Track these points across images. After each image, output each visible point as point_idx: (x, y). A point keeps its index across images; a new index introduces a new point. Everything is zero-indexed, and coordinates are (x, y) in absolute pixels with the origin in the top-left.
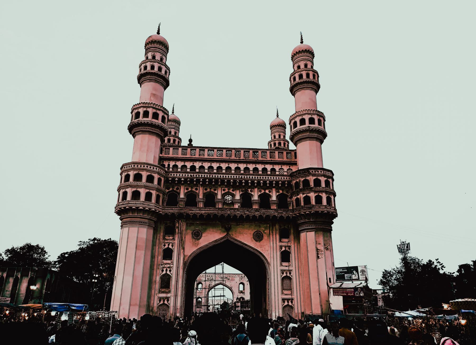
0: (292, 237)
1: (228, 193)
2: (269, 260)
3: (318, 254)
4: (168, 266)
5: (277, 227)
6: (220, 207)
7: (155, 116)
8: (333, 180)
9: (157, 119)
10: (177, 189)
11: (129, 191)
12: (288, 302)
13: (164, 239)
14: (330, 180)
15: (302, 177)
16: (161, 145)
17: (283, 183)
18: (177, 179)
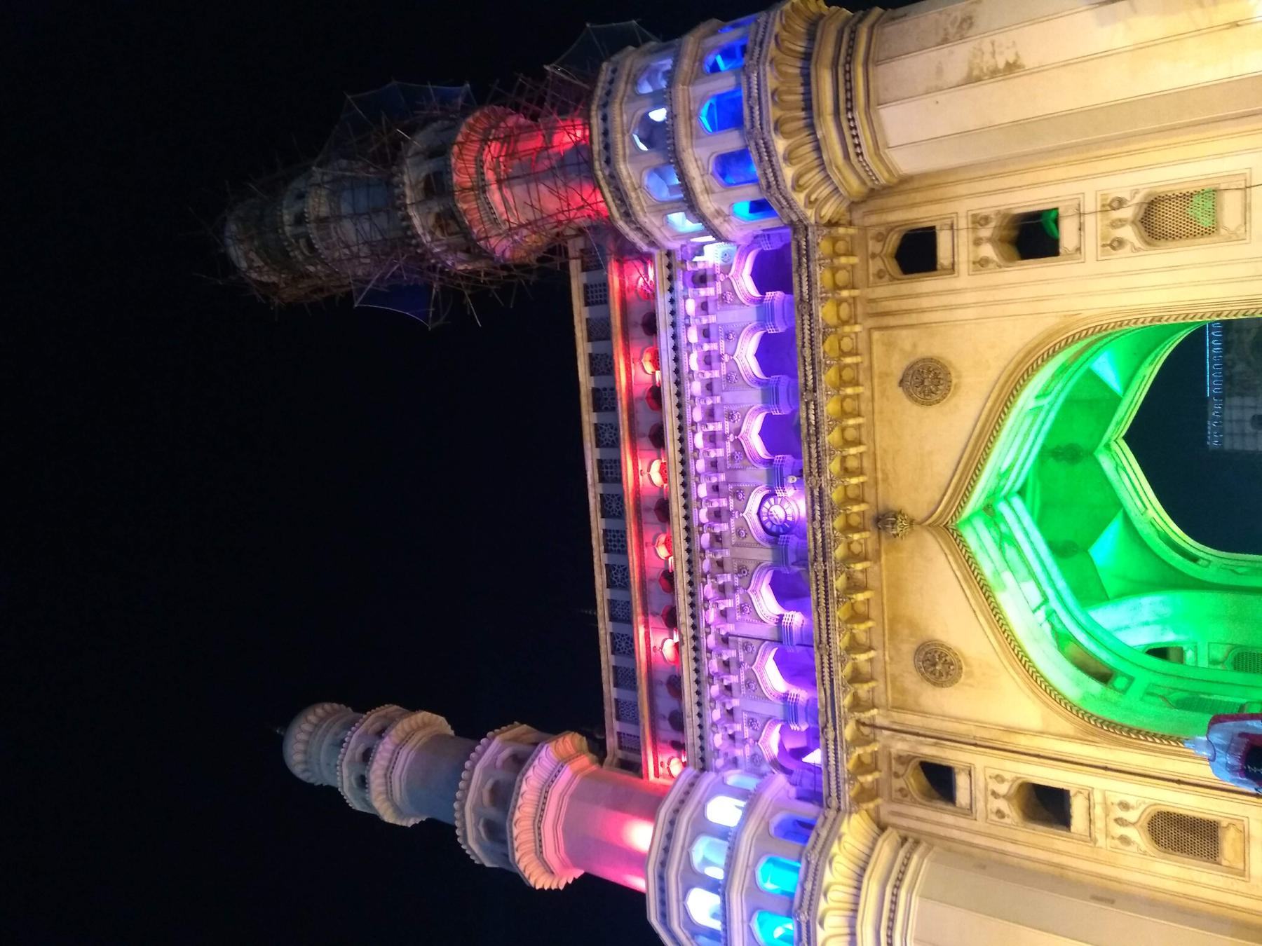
2: (1050, 322)
3: (994, 73)
5: (882, 291)
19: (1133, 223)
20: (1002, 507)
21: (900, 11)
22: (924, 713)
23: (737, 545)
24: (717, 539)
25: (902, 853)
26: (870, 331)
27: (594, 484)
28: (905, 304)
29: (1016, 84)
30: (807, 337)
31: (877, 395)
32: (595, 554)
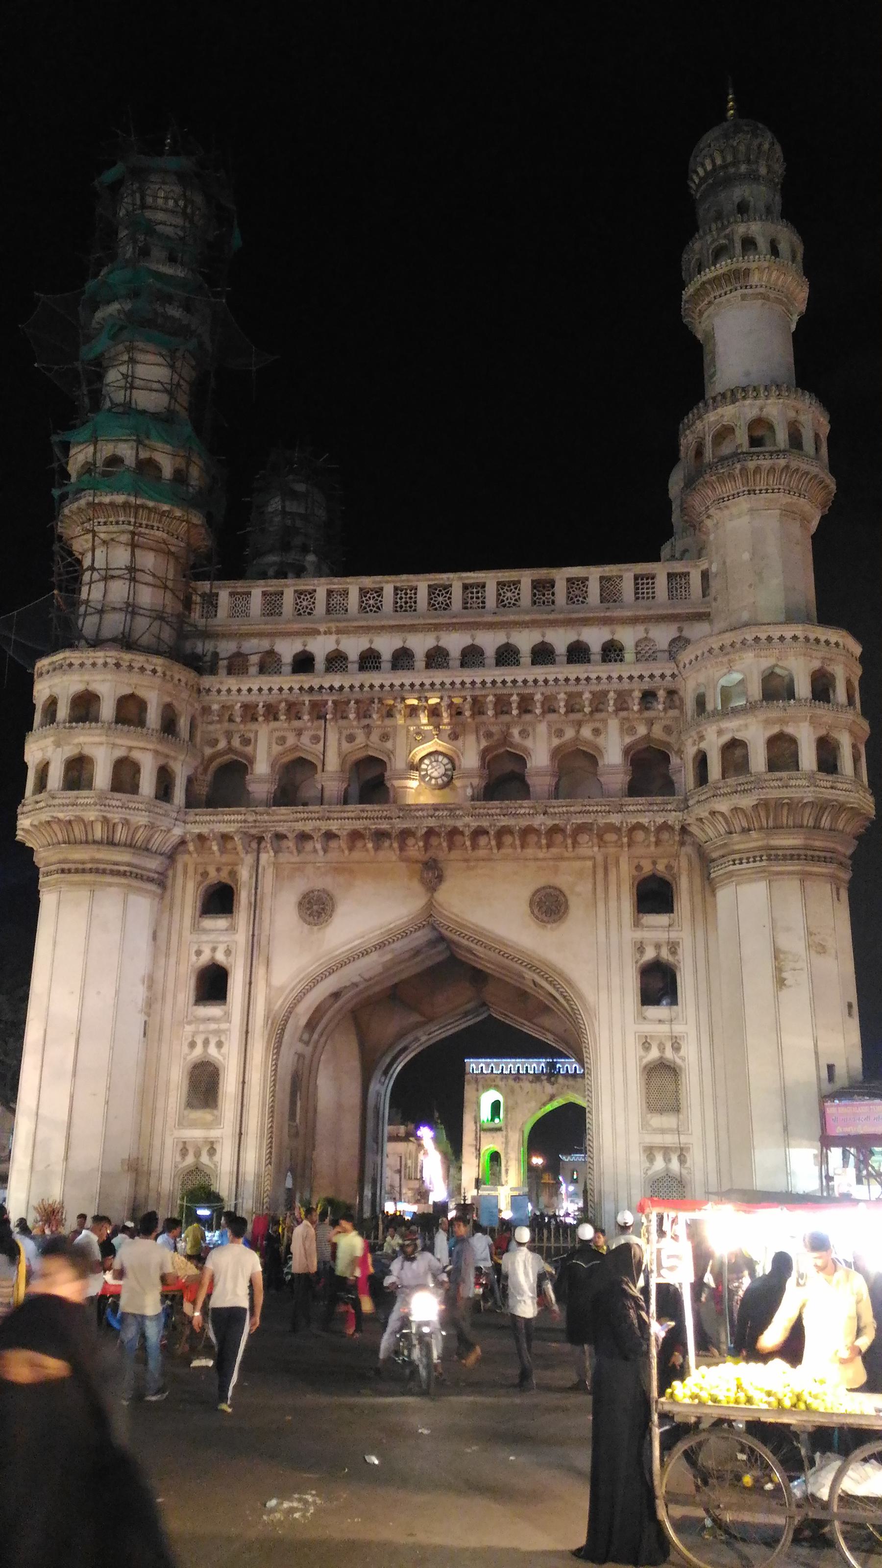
0: (683, 902)
3: (779, 970)
5: (625, 869)
12: (667, 1160)
17: (648, 696)
19: (661, 1057)
20: (441, 947)
21: (844, 895)
22: (274, 895)
23: (408, 731)
24: (413, 711)
25: (156, 876)
26: (593, 858)
27: (461, 578)
28: (613, 889)
30: (591, 809)
31: (539, 863)
32: (393, 578)
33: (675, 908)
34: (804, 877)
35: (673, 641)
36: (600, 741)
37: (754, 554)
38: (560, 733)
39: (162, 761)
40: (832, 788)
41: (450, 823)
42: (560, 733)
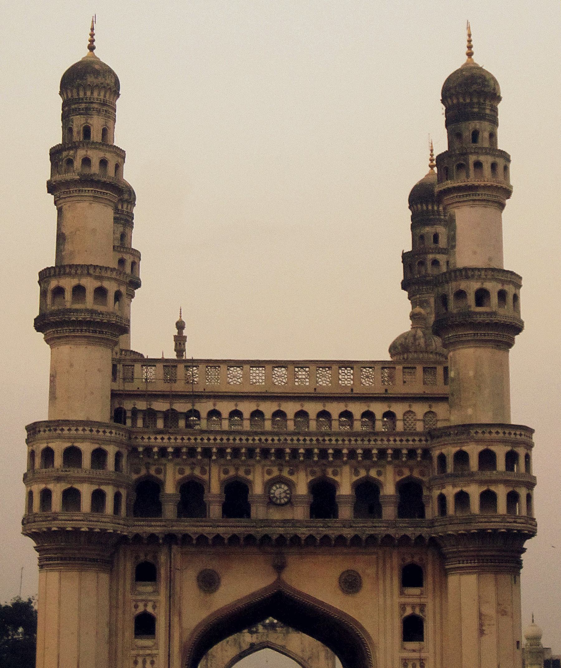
0: (429, 581)
1: (280, 480)
3: (481, 625)
4: (148, 652)
6: (261, 517)
7: (101, 292)
8: (530, 446)
9: (104, 303)
10: (158, 471)
11: (57, 490)
13: (133, 589)
14: (521, 451)
15: (454, 444)
16: (113, 360)
17: (412, 453)
18: (156, 450)
26: (377, 553)
28: (388, 572)
29: (476, 634)
33: (424, 583)
34: (496, 573)
35: (426, 414)
36: (381, 479)
37: (476, 373)
38: (357, 473)
39: (116, 490)
40: (515, 522)
41: (292, 531)
42: (357, 473)
